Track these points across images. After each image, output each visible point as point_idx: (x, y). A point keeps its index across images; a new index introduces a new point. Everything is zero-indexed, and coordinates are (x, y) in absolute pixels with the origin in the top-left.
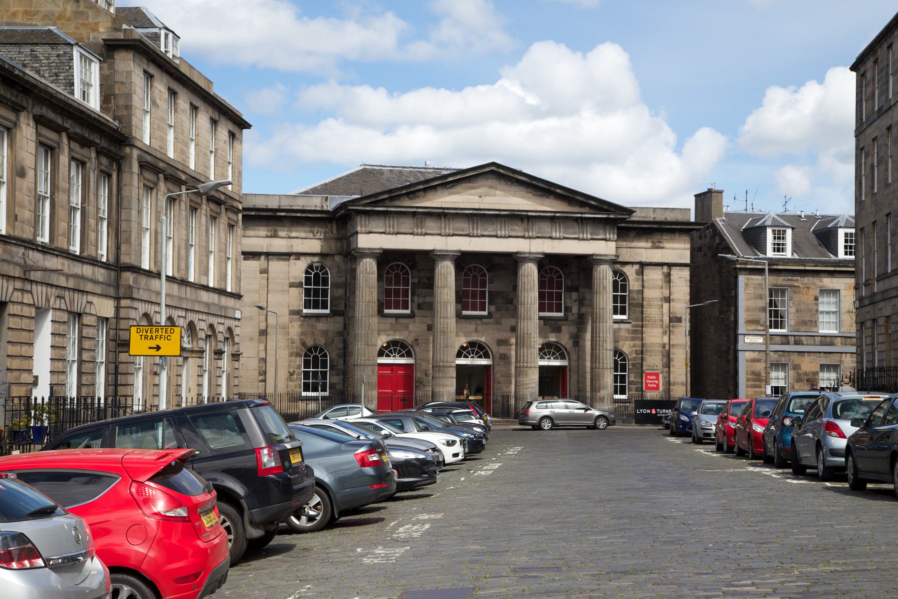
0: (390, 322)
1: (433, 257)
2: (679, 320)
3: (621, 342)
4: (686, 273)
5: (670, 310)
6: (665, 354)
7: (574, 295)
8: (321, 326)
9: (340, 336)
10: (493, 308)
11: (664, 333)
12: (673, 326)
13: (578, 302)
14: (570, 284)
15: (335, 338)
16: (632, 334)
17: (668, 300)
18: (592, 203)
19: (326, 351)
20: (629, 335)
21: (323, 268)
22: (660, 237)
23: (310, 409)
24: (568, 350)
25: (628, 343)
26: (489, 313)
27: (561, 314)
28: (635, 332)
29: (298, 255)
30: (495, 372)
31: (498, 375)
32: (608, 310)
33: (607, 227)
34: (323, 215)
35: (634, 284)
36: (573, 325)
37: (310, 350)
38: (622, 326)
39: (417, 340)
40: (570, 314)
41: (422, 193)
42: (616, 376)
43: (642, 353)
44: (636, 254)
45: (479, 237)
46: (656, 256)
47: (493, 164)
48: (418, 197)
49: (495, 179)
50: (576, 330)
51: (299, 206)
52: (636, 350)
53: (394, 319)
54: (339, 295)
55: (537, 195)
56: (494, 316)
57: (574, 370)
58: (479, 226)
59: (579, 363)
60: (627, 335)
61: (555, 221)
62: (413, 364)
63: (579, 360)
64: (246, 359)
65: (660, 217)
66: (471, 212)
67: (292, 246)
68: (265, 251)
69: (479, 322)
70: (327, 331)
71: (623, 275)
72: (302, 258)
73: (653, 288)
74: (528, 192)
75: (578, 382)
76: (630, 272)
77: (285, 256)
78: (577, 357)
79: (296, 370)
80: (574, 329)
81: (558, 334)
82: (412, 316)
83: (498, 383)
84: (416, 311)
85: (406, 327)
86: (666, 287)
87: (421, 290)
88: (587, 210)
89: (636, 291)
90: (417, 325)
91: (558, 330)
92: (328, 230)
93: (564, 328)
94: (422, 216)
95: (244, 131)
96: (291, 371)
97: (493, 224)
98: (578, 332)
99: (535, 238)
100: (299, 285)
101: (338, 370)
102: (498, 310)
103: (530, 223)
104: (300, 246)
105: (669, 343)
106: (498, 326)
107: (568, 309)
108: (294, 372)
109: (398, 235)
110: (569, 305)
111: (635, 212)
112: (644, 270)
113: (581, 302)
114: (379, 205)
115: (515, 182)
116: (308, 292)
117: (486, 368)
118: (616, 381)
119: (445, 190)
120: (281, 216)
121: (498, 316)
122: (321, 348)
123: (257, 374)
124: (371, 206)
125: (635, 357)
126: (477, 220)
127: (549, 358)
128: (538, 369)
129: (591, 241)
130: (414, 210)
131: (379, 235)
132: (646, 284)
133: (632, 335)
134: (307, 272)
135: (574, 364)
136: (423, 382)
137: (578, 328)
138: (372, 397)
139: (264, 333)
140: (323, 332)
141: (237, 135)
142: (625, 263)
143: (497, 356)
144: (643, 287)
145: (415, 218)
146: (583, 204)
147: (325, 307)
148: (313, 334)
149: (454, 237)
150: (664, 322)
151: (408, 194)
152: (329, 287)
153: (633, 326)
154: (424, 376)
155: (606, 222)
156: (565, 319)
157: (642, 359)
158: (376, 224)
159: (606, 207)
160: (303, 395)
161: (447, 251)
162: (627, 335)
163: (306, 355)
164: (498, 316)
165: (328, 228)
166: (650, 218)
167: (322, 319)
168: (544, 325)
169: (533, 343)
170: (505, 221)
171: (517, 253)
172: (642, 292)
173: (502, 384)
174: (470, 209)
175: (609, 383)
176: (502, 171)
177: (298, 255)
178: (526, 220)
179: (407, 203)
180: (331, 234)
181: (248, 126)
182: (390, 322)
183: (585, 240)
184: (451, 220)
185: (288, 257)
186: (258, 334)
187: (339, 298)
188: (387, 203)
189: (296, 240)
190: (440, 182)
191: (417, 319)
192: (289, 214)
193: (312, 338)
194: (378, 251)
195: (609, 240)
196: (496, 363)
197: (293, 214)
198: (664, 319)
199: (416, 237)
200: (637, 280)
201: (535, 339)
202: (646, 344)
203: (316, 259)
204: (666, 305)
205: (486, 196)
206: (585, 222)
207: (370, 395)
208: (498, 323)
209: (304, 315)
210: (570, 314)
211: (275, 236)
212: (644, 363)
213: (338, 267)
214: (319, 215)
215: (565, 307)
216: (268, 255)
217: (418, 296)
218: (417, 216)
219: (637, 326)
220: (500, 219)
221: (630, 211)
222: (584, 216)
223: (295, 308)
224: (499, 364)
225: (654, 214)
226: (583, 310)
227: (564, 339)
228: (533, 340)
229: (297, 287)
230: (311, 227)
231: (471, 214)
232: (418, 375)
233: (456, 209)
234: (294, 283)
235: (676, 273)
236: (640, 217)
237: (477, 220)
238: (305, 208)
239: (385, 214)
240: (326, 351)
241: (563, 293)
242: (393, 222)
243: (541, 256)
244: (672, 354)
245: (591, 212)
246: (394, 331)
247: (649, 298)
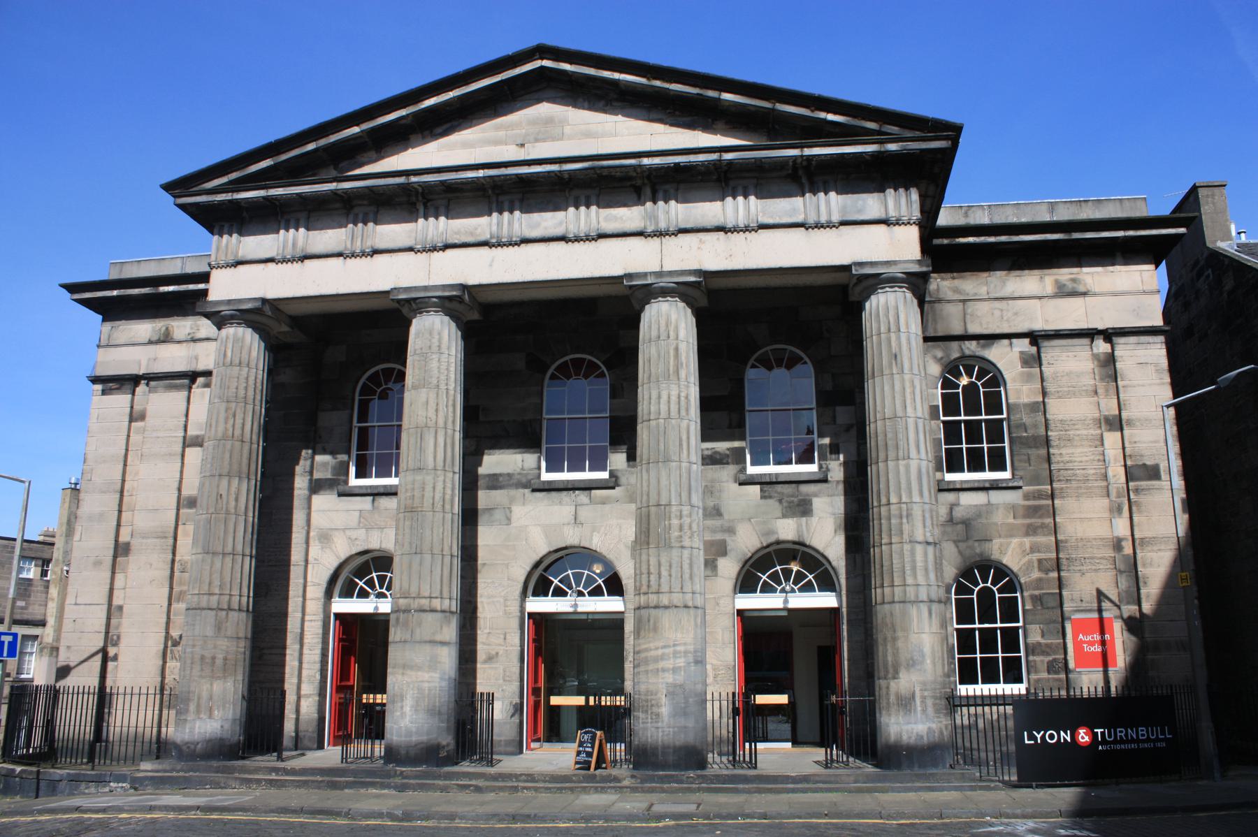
2: (1153, 473)
4: (1156, 352)
5: (1124, 448)
6: (1122, 566)
12: (1137, 491)
16: (1026, 516)
17: (1116, 423)
20: (1020, 521)
25: (1015, 541)
28: (1033, 511)
32: (911, 422)
38: (997, 497)
46: (1072, 315)
52: (1040, 561)
56: (623, 480)
60: (1011, 520)
61: (732, 183)
67: (197, 358)
69: (582, 497)
73: (1072, 393)
86: (1107, 391)
89: (1026, 405)
93: (818, 504)
105: (1133, 535)
108: (181, 637)
109: (307, 262)
112: (1043, 350)
125: (1040, 580)
131: (262, 266)
132: (1050, 387)
138: (211, 698)
144: (1044, 394)
150: (1112, 480)
153: (1027, 497)
162: (1011, 520)
168: (762, 498)
172: (1040, 407)
175: (927, 649)
185: (186, 381)
189: (205, 344)
195: (898, 223)
198: (1110, 474)
200: (1028, 378)
202: (1066, 541)
204: (1112, 438)
205: (537, 140)
207: (205, 695)
211: (166, 338)
212: (1065, 593)
219: (1039, 495)
228: (675, 522)
235: (1127, 351)
246: (367, 529)
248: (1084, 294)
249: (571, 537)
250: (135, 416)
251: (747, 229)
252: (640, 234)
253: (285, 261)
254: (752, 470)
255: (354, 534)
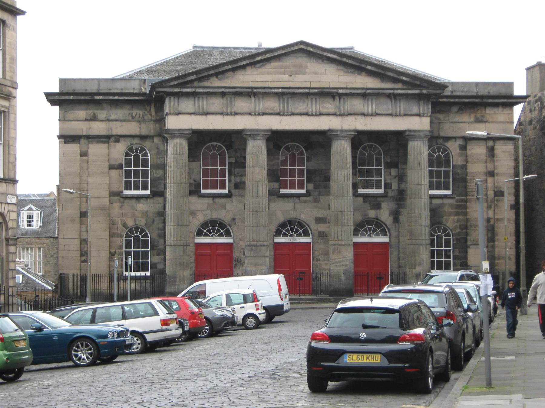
0: (207, 201)
1: (245, 136)
3: (445, 218)
5: (494, 184)
6: (490, 228)
7: (394, 172)
8: (141, 206)
9: (160, 216)
10: (311, 186)
11: (489, 207)
12: (497, 201)
13: (397, 178)
14: (389, 161)
15: (155, 218)
16: (456, 208)
17: (491, 174)
18: (404, 78)
19: (147, 231)
20: (454, 210)
21: (142, 149)
22: (483, 112)
23: (134, 288)
24: (389, 227)
25: (452, 218)
26: (307, 191)
27: (381, 191)
28: (458, 207)
29: (118, 138)
30: (314, 249)
31: (317, 253)
32: (423, 186)
33: (421, 103)
34: (141, 98)
35: (456, 159)
36: (393, 202)
37: (131, 231)
38: (446, 201)
39: (234, 219)
40: (389, 191)
41: (231, 73)
42: (432, 252)
43: (466, 227)
44: (459, 129)
45: (290, 115)
47: (302, 43)
48: (227, 78)
49: (305, 57)
50: (396, 206)
51: (117, 89)
52: (460, 225)
53: (212, 198)
54: (159, 176)
55: (348, 72)
56: (312, 194)
57: (394, 246)
58: (290, 104)
59: (399, 239)
60: (450, 210)
61: (367, 97)
62: (232, 243)
63: (399, 236)
64: (67, 240)
65: (483, 92)
66: (280, 90)
67: (111, 129)
68: (84, 134)
69: (297, 200)
70: (147, 212)
71: (447, 151)
72: (122, 140)
74: (339, 70)
75: (399, 259)
76: (453, 147)
77: (105, 139)
78: (397, 233)
79: (117, 251)
80: (393, 205)
81: (378, 211)
82: (229, 196)
83: (317, 260)
84: (233, 191)
85: (224, 207)
86: (490, 161)
87: (238, 169)
88: (400, 86)
89: (459, 166)
90: (234, 204)
91: (378, 206)
92: (146, 112)
93: (384, 205)
94: (231, 96)
95: (19, 17)
96: (113, 251)
97: (304, 102)
98: (398, 208)
99: (347, 115)
100: (120, 167)
101: (159, 249)
102: (316, 187)
103: (342, 100)
104: (119, 129)
105: (494, 217)
106: (316, 204)
107: (387, 186)
108: (115, 252)
110: (388, 181)
111: (447, 87)
112: (468, 144)
113: (402, 178)
114: (188, 86)
115: (326, 60)
116: (128, 174)
117: (307, 245)
118: (432, 256)
119: (254, 69)
120: (100, 100)
121: (316, 193)
122: (141, 228)
123: (79, 255)
124: (178, 88)
125: (459, 232)
126: (288, 98)
127: (369, 235)
128: (352, 247)
129: (405, 117)
130: (223, 90)
131: (189, 116)
132: (469, 159)
133: (456, 210)
134: (127, 155)
135: (394, 240)
136: (241, 261)
137: (398, 204)
138: (184, 277)
139: (84, 215)
140: (143, 213)
141: (7, 22)
142: (448, 139)
143: (316, 234)
144: (467, 161)
145: (225, 99)
146: (395, 80)
147: (145, 188)
148: (133, 214)
149: (265, 117)
150: (489, 196)
151: (216, 75)
152: (149, 168)
153: (457, 201)
154: (242, 255)
155: (419, 98)
156: (385, 195)
157: (467, 234)
158: (187, 105)
159: (418, 83)
160: (124, 275)
161: (257, 130)
162: (450, 210)
163: (127, 236)
164: (316, 193)
165: (146, 110)
166: (472, 92)
167: (142, 201)
168: (363, 202)
169: (346, 221)
170: (316, 99)
171: (329, 130)
172: (464, 167)
173: (321, 262)
174: (279, 88)
175: (425, 260)
176: (311, 49)
177: (118, 138)
178: (337, 98)
179: (215, 82)
180: (150, 116)
181: (23, 13)
182: (207, 201)
183: (398, 116)
184: (261, 99)
185: (107, 139)
186: (79, 216)
187: (159, 179)
188: (196, 84)
189: (114, 123)
190: (248, 62)
191: (234, 199)
192: (107, 98)
193: (132, 218)
194: (187, 132)
195: (423, 116)
196: (314, 241)
197: (111, 98)
198: (489, 193)
199: (226, 117)
200: (461, 155)
201: (349, 216)
202: (470, 219)
203: (136, 141)
204: (490, 180)
205: (296, 74)
206: (398, 98)
207: (182, 276)
208: (316, 201)
209: (124, 196)
210: (389, 191)
211: (94, 118)
212: (468, 238)
213: (158, 148)
214: (136, 98)
215: (385, 184)
216: (90, 138)
217: (235, 176)
218: (227, 96)
219: (461, 201)
220: (311, 97)
221: (442, 86)
222: (396, 92)
223: (115, 189)
224: (318, 242)
225: (476, 89)
226: (403, 186)
227: (385, 215)
228: (346, 217)
229: (117, 169)
230: (129, 110)
231: (280, 92)
232: (235, 254)
233: (264, 88)
234: (114, 165)
236: (462, 92)
237: (288, 98)
238: (124, 91)
239: (194, 95)
240: (147, 231)
241: (383, 170)
242: (203, 102)
243: (353, 133)
244: (497, 228)
245: (404, 87)
247: (473, 173)
248: (486, 122)
249: (292, 215)
250: (83, 154)
251: (372, 115)
252: (335, 114)
253: (199, 114)
254: (360, 191)
255: (206, 212)
